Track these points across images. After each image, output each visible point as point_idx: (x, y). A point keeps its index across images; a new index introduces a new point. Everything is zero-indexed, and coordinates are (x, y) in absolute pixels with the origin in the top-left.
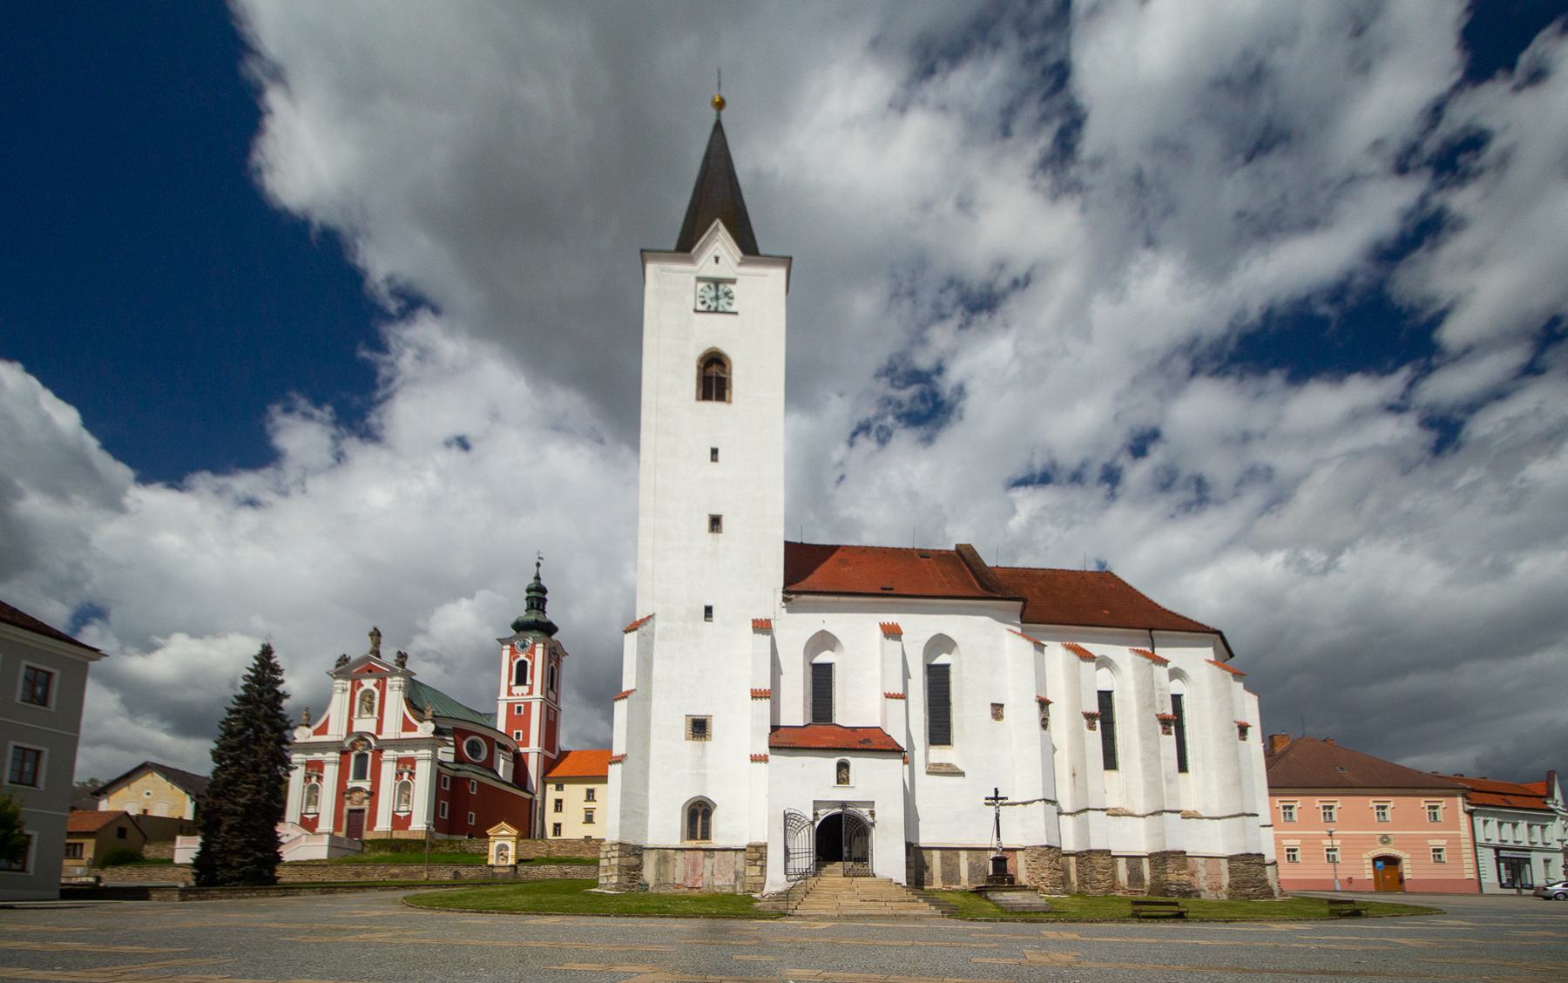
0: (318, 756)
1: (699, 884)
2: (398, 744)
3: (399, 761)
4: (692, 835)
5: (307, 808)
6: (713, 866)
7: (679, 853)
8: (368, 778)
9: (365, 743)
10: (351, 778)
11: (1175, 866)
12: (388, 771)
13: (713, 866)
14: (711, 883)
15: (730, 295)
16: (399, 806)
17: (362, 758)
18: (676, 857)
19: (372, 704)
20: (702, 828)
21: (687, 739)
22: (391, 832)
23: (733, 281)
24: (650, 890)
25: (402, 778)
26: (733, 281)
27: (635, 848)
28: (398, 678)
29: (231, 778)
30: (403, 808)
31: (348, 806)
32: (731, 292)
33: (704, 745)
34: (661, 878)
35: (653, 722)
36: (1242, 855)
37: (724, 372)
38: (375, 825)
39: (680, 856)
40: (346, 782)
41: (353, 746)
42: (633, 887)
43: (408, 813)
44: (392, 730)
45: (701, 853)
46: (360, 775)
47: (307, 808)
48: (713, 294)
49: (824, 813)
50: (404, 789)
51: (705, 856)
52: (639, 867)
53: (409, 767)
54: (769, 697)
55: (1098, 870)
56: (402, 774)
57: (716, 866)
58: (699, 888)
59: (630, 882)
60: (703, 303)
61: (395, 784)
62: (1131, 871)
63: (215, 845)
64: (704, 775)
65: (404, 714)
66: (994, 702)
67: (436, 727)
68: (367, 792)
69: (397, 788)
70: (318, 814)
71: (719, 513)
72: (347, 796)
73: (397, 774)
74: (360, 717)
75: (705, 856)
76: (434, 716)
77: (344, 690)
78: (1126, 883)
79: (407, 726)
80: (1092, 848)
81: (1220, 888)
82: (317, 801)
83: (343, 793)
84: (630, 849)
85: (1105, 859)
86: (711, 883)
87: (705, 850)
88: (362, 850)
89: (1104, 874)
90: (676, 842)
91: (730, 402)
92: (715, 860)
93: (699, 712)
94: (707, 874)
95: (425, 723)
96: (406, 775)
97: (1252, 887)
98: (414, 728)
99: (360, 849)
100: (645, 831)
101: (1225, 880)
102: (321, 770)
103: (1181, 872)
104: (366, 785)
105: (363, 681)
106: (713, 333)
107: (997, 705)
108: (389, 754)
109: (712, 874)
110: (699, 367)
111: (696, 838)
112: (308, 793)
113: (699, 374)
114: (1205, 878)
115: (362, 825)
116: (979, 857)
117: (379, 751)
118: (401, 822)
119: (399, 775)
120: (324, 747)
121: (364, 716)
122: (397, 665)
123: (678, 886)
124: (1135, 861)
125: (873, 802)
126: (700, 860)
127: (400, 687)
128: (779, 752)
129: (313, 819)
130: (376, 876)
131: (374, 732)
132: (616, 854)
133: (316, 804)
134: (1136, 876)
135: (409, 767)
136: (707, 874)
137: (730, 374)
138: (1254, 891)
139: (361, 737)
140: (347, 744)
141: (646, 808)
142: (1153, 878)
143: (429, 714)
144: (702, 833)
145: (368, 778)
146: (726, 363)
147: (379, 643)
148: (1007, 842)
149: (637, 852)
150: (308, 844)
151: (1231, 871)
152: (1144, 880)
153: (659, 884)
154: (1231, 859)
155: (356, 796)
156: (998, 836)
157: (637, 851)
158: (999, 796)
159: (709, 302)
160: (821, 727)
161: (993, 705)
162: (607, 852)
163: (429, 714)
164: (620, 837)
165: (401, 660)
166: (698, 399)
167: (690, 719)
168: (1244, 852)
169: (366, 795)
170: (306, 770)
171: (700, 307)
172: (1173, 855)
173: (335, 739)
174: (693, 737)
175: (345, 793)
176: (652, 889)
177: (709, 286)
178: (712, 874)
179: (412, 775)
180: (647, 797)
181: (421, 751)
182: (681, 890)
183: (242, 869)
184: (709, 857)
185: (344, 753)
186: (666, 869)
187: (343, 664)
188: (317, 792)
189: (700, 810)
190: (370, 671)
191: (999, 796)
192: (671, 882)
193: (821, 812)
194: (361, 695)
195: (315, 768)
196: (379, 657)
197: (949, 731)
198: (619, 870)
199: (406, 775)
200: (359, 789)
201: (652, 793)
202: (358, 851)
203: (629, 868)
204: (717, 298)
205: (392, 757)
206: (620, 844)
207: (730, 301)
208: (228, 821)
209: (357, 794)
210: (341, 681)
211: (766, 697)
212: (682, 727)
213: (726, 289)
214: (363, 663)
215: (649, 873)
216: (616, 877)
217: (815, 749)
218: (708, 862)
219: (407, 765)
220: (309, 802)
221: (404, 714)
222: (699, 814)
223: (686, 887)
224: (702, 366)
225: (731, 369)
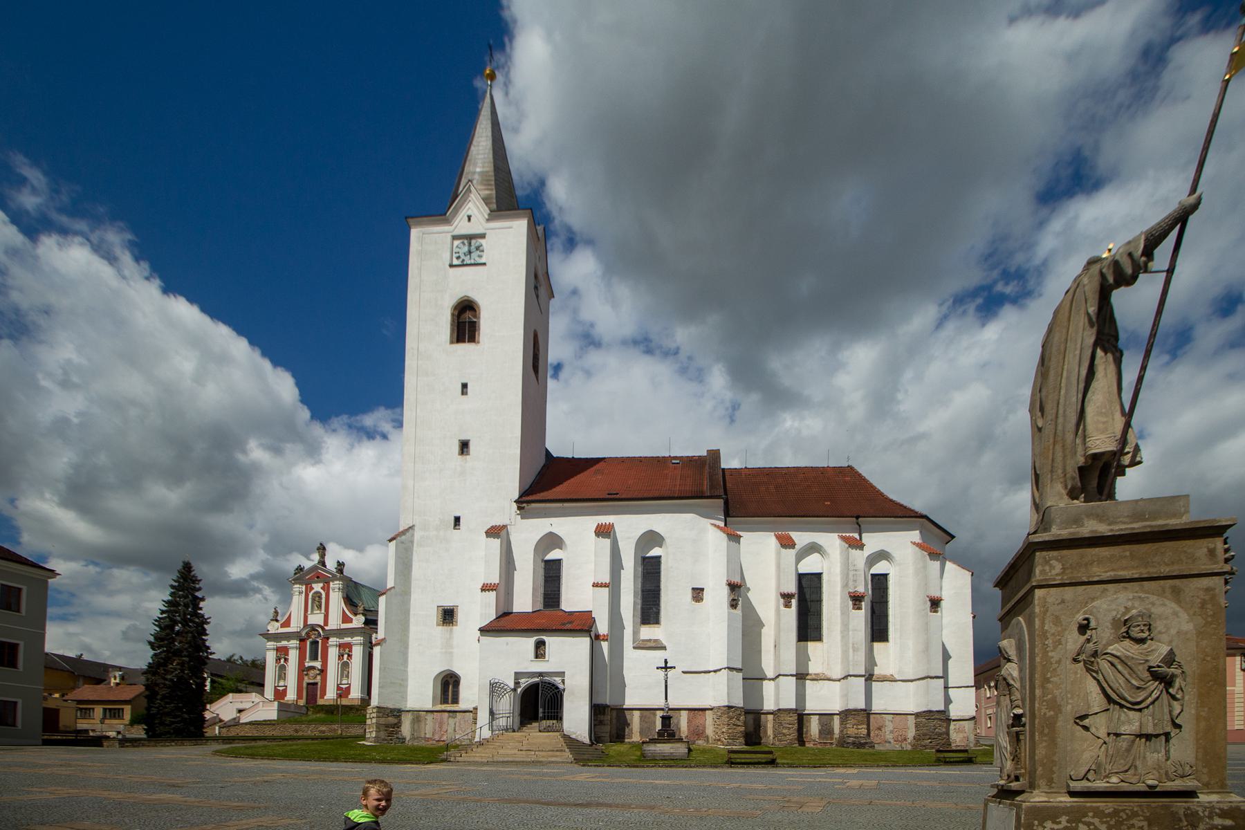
0: (284, 643)
1: (444, 738)
2: (340, 633)
3: (340, 646)
4: (444, 700)
5: (278, 682)
6: (455, 724)
7: (429, 714)
8: (319, 659)
9: (316, 632)
10: (307, 660)
11: (856, 721)
12: (333, 653)
13: (455, 724)
14: (453, 737)
15: (481, 248)
16: (341, 680)
17: (315, 643)
19: (320, 602)
20: (453, 695)
21: (438, 625)
22: (297, 701)
23: (483, 236)
24: (407, 742)
25: (343, 659)
26: (483, 236)
27: (392, 710)
28: (338, 582)
29: (162, 661)
30: (344, 682)
31: (306, 680)
32: (482, 245)
33: (451, 630)
35: (412, 612)
36: (924, 712)
37: (475, 316)
38: (286, 696)
39: (429, 717)
40: (304, 663)
41: (307, 634)
42: (391, 740)
43: (347, 686)
44: (335, 622)
45: (446, 714)
46: (314, 658)
47: (278, 682)
48: (466, 249)
49: (525, 682)
50: (345, 667)
52: (398, 725)
53: (347, 650)
54: (495, 590)
56: (343, 656)
57: (457, 724)
58: (444, 741)
60: (458, 258)
61: (338, 664)
62: (822, 726)
63: (153, 709)
64: (451, 653)
65: (343, 609)
67: (366, 619)
68: (319, 670)
69: (340, 666)
70: (286, 686)
71: (468, 439)
72: (305, 673)
73: (339, 656)
74: (312, 613)
75: (449, 717)
76: (365, 610)
78: (817, 736)
79: (346, 619)
80: (781, 708)
81: (905, 740)
82: (285, 677)
83: (303, 670)
84: (389, 711)
85: (791, 717)
86: (453, 737)
87: (449, 712)
88: (307, 713)
89: (789, 729)
90: (429, 706)
91: (478, 342)
93: (448, 603)
94: (450, 730)
95: (358, 616)
96: (346, 656)
97: (929, 738)
98: (350, 621)
99: (305, 712)
100: (404, 698)
101: (911, 733)
103: (859, 727)
104: (318, 664)
105: (314, 585)
106: (464, 283)
108: (333, 641)
109: (455, 731)
110: (453, 315)
111: (448, 703)
112: (279, 670)
113: (453, 321)
114: (892, 732)
115: (317, 695)
118: (343, 692)
119: (341, 656)
120: (288, 636)
121: (315, 612)
122: (337, 572)
123: (427, 739)
124: (825, 717)
125: (564, 672)
126: (445, 720)
127: (339, 589)
128: (487, 633)
129: (283, 690)
130: (309, 732)
131: (322, 625)
132: (375, 715)
133: (285, 680)
134: (826, 731)
135: (347, 650)
136: (450, 730)
137: (479, 318)
138: (931, 742)
139: (313, 628)
140: (303, 634)
141: (405, 680)
142: (841, 731)
143: (360, 609)
144: (453, 699)
145: (319, 659)
146: (477, 310)
147: (325, 555)
148: (673, 703)
150: (264, 708)
151: (917, 726)
152: (833, 734)
153: (413, 738)
154: (917, 715)
155: (312, 673)
156: (666, 698)
157: (397, 713)
158: (668, 665)
159: (463, 257)
160: (549, 612)
162: (371, 713)
163: (360, 609)
164: (379, 703)
165: (339, 568)
166: (452, 342)
167: (441, 609)
168: (926, 709)
169: (318, 672)
170: (277, 654)
171: (456, 262)
172: (853, 713)
173: (295, 630)
174: (444, 623)
175: (303, 671)
176: (408, 742)
177: (463, 243)
178: (455, 731)
179: (350, 656)
180: (407, 671)
181: (355, 638)
182: (431, 742)
183: (173, 726)
185: (302, 640)
186: (419, 727)
187: (299, 573)
188: (285, 670)
189: (451, 681)
190: (319, 578)
191: (668, 665)
192: (423, 736)
193: (522, 681)
194: (312, 596)
195: (282, 653)
196: (325, 566)
198: (377, 727)
199: (346, 656)
200: (313, 668)
201: (411, 668)
202: (303, 714)
204: (470, 252)
205: (335, 643)
206: (377, 707)
207: (481, 253)
208: (164, 692)
209: (312, 672)
210: (298, 586)
211: (492, 590)
212: (434, 616)
213: (477, 244)
214: (313, 571)
216: (374, 733)
218: (451, 721)
219: (346, 649)
220: (280, 678)
221: (343, 609)
222: (449, 684)
223: (434, 740)
224: (456, 313)
225: (480, 313)
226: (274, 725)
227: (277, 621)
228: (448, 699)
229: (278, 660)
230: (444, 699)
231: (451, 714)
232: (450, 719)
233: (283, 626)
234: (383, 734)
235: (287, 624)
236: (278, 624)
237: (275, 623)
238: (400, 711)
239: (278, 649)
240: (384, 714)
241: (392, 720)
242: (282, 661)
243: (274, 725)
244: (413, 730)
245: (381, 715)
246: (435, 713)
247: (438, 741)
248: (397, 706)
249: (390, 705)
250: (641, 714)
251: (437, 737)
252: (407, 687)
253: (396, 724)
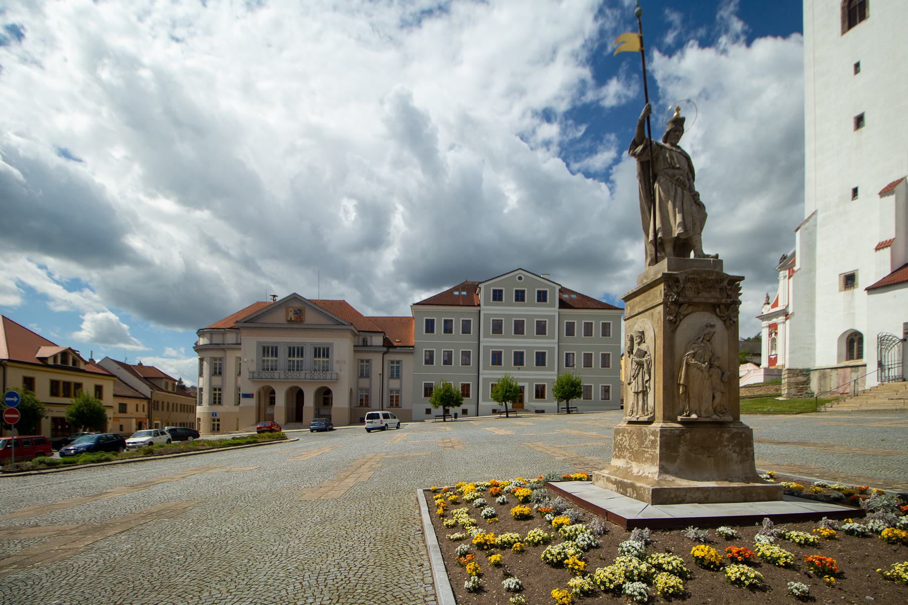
4: (850, 357)
7: (834, 370)
18: (831, 374)
27: (801, 371)
34: (822, 389)
39: (834, 373)
45: (849, 369)
51: (852, 371)
52: (807, 382)
58: (847, 393)
59: (799, 392)
77: (785, 277)
84: (798, 371)
87: (852, 367)
90: (834, 364)
92: (859, 373)
102: (776, 329)
126: (848, 375)
141: (813, 344)
149: (804, 373)
157: (806, 373)
184: (855, 371)
203: (797, 384)
215: (814, 386)
223: (838, 393)
226: (760, 386)
227: (768, 304)
228: (853, 355)
229: (770, 334)
230: (850, 355)
231: (854, 369)
232: (853, 373)
233: (773, 307)
234: (793, 391)
235: (776, 305)
236: (769, 307)
237: (767, 306)
238: (809, 370)
239: (770, 326)
240: (794, 374)
241: (801, 379)
242: (773, 334)
243: (760, 386)
244: (820, 385)
245: (791, 375)
246: (839, 370)
247: (843, 394)
248: (806, 366)
249: (800, 366)
251: (841, 390)
252: (814, 349)
253: (805, 382)
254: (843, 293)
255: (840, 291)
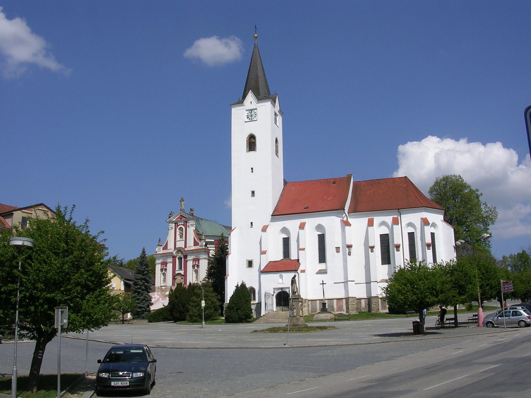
2: (192, 252)
46: (180, 268)
55: (374, 303)
65: (194, 238)
66: (336, 247)
79: (196, 244)
85: (376, 300)
89: (375, 305)
107: (337, 248)
108: (190, 258)
116: (331, 302)
117: (185, 257)
145: (183, 269)
148: (327, 296)
156: (324, 296)
158: (324, 283)
161: (336, 248)
191: (324, 283)
193: (275, 291)
197: (325, 258)
217: (270, 272)
250: (320, 302)
254: (248, 268)
255: (247, 268)
